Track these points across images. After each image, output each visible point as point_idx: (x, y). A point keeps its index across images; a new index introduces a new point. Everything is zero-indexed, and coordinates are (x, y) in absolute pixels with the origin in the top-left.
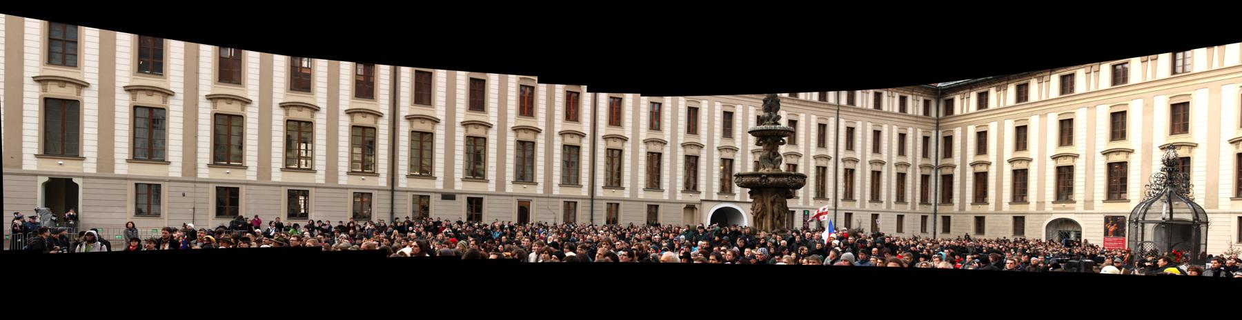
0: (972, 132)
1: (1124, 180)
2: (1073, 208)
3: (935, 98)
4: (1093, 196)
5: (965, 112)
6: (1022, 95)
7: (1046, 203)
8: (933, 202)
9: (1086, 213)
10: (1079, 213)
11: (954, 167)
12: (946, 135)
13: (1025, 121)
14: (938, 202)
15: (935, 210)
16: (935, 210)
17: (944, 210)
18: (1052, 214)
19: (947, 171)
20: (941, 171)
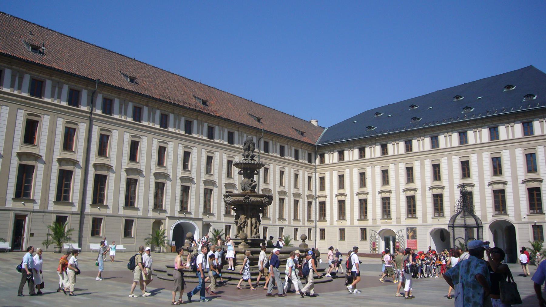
0: (335, 174)
1: (504, 201)
2: (391, 223)
3: (314, 152)
4: (400, 217)
5: (331, 162)
6: (409, 148)
7: (377, 220)
8: (314, 220)
9: (397, 226)
10: (394, 226)
13: (364, 170)
14: (317, 220)
17: (321, 225)
18: (380, 226)
19: (322, 199)
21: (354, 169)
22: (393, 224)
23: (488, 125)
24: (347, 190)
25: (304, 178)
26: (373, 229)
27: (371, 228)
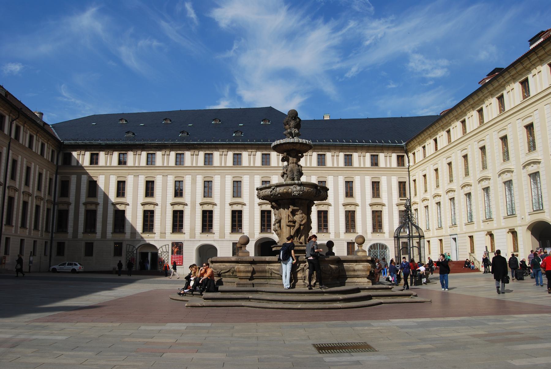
2: (154, 237)
9: (161, 241)
14: (54, 231)
15: (52, 237)
22: (156, 239)
26: (131, 244)
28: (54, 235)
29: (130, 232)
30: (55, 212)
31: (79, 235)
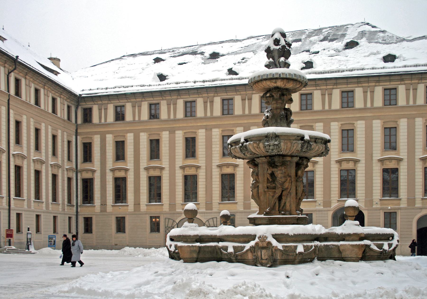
0: (110, 139)
7: (177, 205)
9: (207, 213)
11: (94, 171)
12: (85, 142)
14: (79, 204)
15: (77, 212)
16: (77, 212)
20: (81, 175)
21: (142, 134)
23: (341, 88)
24: (130, 164)
25: (63, 141)
27: (168, 216)
28: (79, 209)
29: (168, 202)
30: (79, 181)
31: (108, 209)
